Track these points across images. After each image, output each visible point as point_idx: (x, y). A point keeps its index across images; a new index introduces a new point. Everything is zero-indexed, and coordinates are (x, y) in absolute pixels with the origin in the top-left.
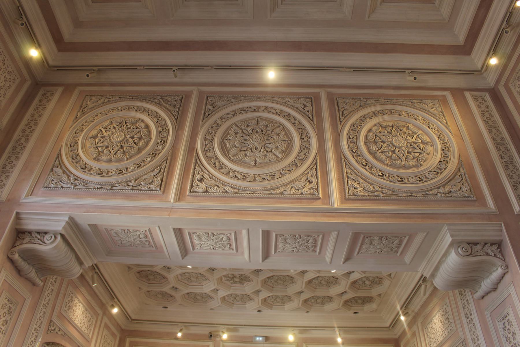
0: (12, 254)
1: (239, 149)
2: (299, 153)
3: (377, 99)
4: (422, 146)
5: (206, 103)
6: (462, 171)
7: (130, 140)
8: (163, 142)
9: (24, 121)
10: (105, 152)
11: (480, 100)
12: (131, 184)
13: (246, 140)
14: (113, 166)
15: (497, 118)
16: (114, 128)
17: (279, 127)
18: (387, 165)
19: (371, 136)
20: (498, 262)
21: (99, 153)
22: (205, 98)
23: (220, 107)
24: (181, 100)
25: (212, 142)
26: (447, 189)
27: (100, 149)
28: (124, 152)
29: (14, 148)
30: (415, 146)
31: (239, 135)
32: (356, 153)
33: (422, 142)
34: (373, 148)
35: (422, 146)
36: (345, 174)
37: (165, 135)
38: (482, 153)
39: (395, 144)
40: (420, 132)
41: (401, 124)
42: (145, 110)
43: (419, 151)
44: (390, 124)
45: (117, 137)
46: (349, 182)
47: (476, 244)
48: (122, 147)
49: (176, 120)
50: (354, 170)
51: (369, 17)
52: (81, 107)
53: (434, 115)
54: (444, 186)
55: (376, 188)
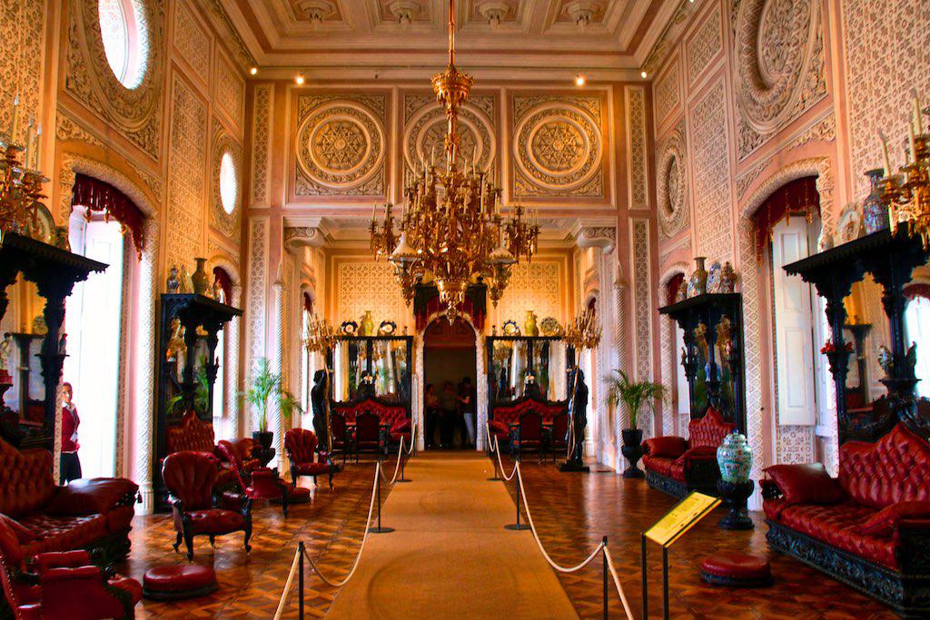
5: (406, 106)
6: (600, 173)
9: (254, 128)
11: (635, 96)
12: (361, 189)
14: (343, 173)
15: (643, 118)
16: (335, 134)
18: (546, 167)
19: (538, 140)
20: (611, 240)
21: (330, 161)
26: (585, 189)
27: (329, 156)
29: (257, 157)
33: (577, 145)
34: (538, 151)
35: (575, 148)
38: (620, 152)
40: (577, 134)
42: (355, 113)
45: (340, 145)
47: (599, 228)
48: (346, 155)
50: (521, 173)
53: (591, 115)
55: (536, 189)
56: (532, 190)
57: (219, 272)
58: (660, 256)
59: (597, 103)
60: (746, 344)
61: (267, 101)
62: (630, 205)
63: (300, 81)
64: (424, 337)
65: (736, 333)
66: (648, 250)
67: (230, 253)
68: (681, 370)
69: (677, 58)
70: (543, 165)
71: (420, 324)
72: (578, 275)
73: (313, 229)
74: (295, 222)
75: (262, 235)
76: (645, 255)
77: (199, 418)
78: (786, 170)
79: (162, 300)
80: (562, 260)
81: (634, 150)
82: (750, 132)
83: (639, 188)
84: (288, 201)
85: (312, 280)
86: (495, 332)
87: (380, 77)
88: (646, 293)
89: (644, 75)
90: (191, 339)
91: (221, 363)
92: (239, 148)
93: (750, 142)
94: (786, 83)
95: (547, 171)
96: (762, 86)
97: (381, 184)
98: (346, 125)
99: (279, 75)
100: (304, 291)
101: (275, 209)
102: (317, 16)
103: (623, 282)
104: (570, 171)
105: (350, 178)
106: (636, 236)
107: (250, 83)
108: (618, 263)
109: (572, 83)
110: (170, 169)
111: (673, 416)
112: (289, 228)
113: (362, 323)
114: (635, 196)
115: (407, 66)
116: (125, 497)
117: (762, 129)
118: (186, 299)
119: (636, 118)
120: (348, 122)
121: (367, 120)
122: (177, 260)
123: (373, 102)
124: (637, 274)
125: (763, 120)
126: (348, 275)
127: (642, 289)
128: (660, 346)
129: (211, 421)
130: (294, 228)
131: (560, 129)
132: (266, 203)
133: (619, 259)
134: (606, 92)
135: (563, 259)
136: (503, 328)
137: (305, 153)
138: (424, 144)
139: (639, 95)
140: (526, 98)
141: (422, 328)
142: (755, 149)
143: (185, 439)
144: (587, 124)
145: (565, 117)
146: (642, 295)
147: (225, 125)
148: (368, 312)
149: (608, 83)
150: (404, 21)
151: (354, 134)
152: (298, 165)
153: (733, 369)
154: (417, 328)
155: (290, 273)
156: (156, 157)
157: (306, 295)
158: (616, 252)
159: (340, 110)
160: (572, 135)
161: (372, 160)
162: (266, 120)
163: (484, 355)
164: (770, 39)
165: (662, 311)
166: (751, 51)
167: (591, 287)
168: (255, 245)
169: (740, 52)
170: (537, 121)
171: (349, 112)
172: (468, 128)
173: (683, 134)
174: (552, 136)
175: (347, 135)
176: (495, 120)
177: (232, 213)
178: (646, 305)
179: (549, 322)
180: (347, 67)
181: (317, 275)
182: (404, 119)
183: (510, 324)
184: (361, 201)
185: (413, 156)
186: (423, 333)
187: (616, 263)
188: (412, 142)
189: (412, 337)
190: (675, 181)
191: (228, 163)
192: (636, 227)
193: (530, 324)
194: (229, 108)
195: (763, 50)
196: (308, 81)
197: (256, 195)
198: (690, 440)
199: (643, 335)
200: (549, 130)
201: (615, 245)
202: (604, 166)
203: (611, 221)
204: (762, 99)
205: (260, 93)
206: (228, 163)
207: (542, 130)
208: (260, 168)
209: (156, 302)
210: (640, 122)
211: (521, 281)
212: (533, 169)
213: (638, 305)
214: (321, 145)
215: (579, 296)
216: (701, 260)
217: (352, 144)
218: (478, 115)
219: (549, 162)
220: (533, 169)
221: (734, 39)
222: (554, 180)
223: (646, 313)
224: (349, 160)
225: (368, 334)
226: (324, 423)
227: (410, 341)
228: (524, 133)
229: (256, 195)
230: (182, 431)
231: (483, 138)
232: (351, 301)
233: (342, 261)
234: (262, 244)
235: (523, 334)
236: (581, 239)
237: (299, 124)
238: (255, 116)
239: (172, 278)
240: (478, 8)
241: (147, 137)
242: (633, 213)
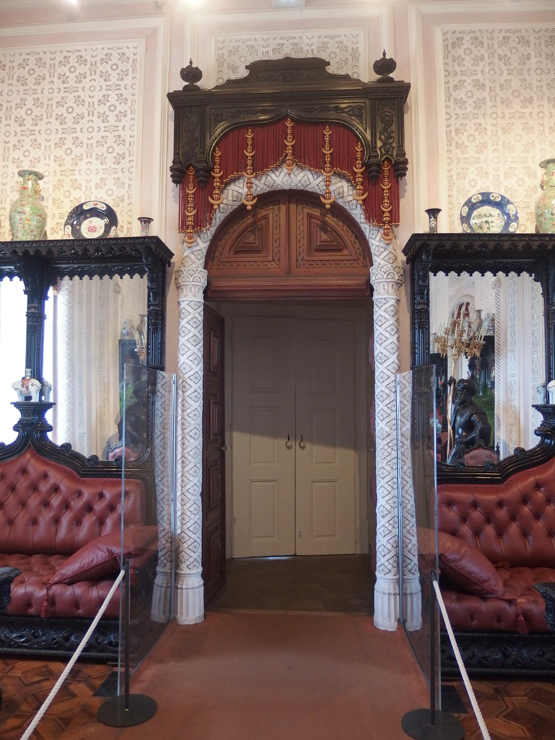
71: (191, 213)
163: (397, 312)
186: (202, 244)
211: (515, 84)
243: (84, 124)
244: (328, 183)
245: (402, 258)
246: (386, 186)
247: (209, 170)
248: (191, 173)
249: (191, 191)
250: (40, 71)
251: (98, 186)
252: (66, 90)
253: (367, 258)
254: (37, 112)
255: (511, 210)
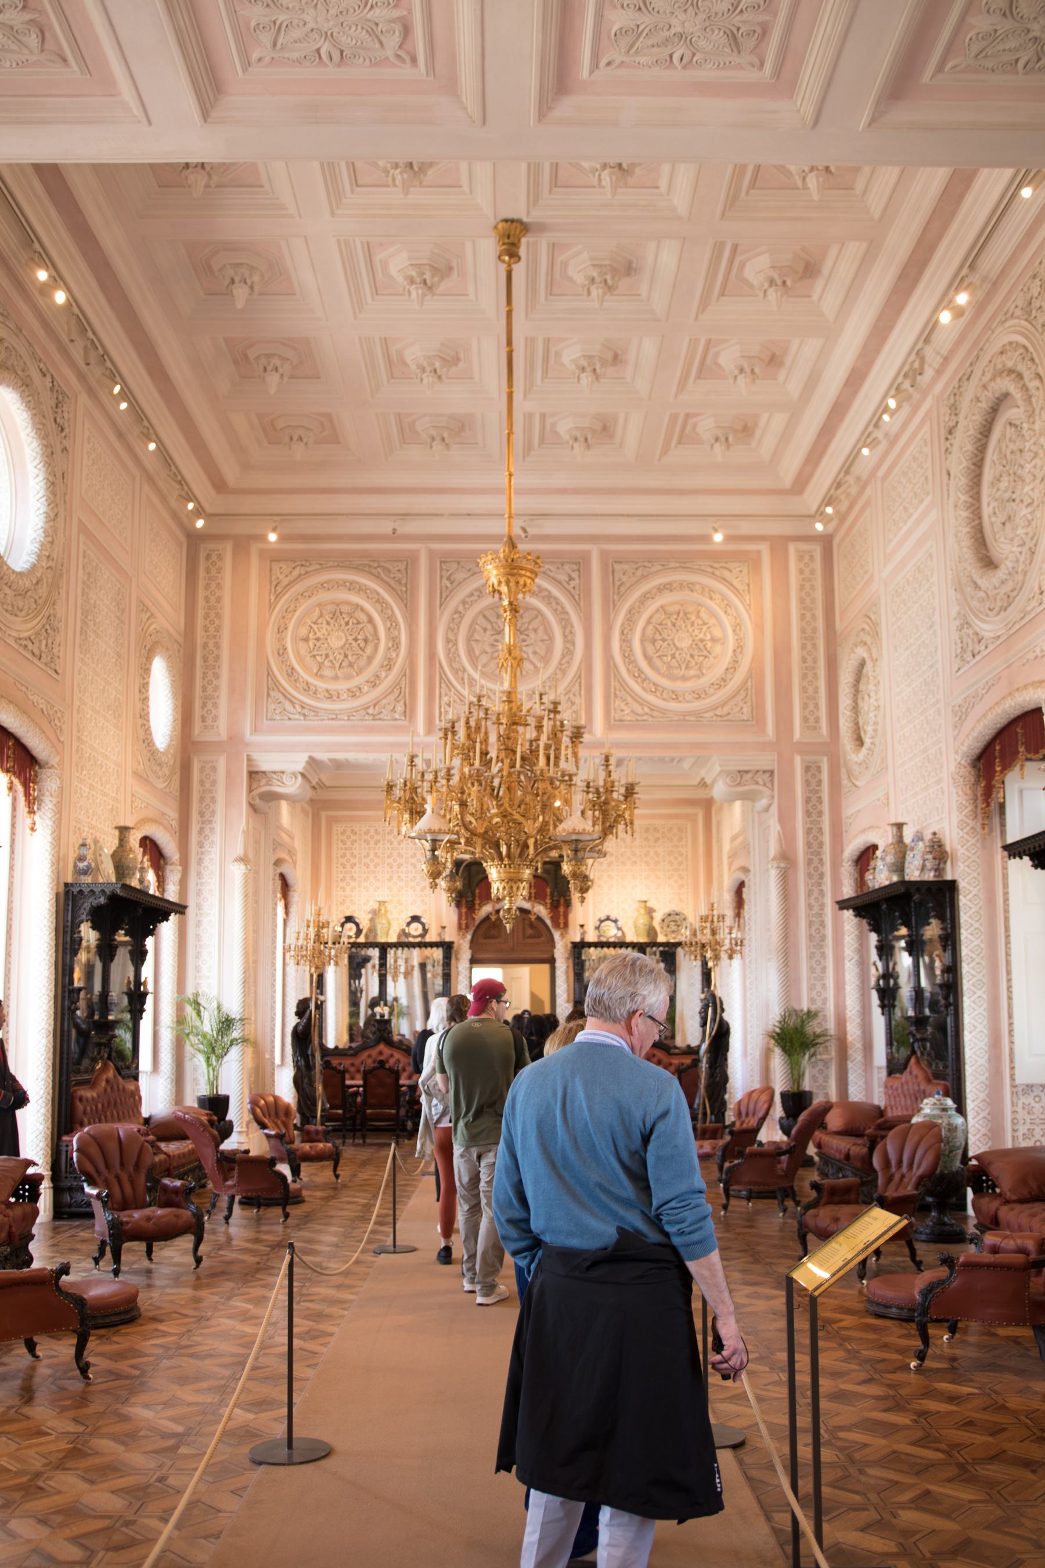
0: (253, 799)
1: (489, 655)
2: (562, 659)
3: (664, 561)
4: (709, 645)
5: (441, 577)
6: (749, 683)
7: (354, 644)
8: (397, 646)
9: (200, 613)
10: (327, 663)
11: (806, 558)
12: (371, 711)
13: (497, 641)
14: (342, 686)
15: (819, 594)
16: (328, 623)
17: (537, 617)
18: (663, 675)
20: (767, 791)
21: (321, 666)
22: (438, 564)
23: (460, 583)
24: (406, 569)
25: (456, 644)
26: (726, 710)
27: (319, 658)
28: (351, 665)
29: (205, 659)
30: (701, 645)
31: (488, 633)
32: (628, 657)
33: (714, 640)
36: (613, 690)
37: (396, 633)
39: (677, 644)
40: (713, 621)
41: (690, 609)
42: (361, 589)
43: (705, 653)
44: (676, 608)
45: (337, 640)
46: (617, 703)
47: (747, 772)
48: (346, 656)
49: (406, 605)
51: (660, 460)
52: (271, 583)
54: (722, 706)
55: (647, 710)
56: (639, 710)
57: (149, 844)
58: (844, 816)
59: (745, 571)
60: (964, 959)
61: (219, 570)
62: (797, 735)
63: (273, 537)
64: (472, 941)
65: (950, 940)
66: (826, 807)
67: (163, 814)
68: (874, 996)
69: (867, 503)
70: (659, 673)
71: (464, 922)
72: (719, 841)
73: (294, 774)
74: (266, 762)
75: (214, 783)
76: (820, 814)
77: (120, 1074)
78: (1016, 694)
79: (67, 893)
80: (693, 818)
81: (803, 647)
82: (970, 632)
83: (811, 706)
84: (255, 730)
85: (291, 852)
86: (583, 934)
87: (399, 531)
88: (822, 876)
89: (819, 527)
90: (106, 951)
91: (150, 987)
92: (176, 646)
93: (970, 648)
94: (1017, 561)
95: (663, 682)
96: (988, 563)
97: (402, 703)
98: (345, 608)
99: (241, 528)
100: (279, 871)
101: (235, 740)
102: (300, 439)
103: (786, 859)
104: (703, 680)
105: (353, 694)
106: (807, 783)
107: (194, 540)
108: (778, 828)
109: (707, 539)
110: (76, 688)
111: (865, 1070)
112: (257, 773)
113: (372, 920)
114: (805, 720)
115: (442, 515)
116: (25, 1190)
117: (988, 628)
118: (103, 891)
119: (808, 594)
120: (348, 603)
121: (379, 601)
122: (86, 829)
123: (389, 571)
124: (809, 845)
125: (987, 615)
126: (348, 843)
127: (816, 869)
128: (844, 959)
129: (136, 1078)
130: (264, 773)
131: (685, 614)
132: (222, 730)
133: (781, 820)
134: (759, 552)
135: (696, 815)
136: (597, 928)
137: (282, 652)
138: (469, 639)
139: (812, 558)
140: (629, 565)
141: (467, 927)
142: (978, 658)
143: (100, 1105)
144: (728, 606)
145: (695, 594)
146: (816, 877)
147: (153, 609)
148: (382, 903)
149: (763, 538)
150: (437, 446)
151: (359, 623)
152: (270, 673)
153: (946, 998)
154: (460, 927)
155: (257, 842)
156: (56, 671)
157: (282, 877)
158: (774, 809)
159: (339, 585)
160: (705, 624)
161: (389, 665)
162: (219, 600)
163: (567, 972)
164: (998, 490)
165: (843, 905)
166: (972, 505)
167: (739, 862)
168: (202, 799)
169: (956, 506)
170: (649, 602)
171: (351, 586)
172: (539, 612)
173: (875, 625)
174: (674, 625)
175: (347, 624)
176: (581, 598)
177: (169, 746)
178: (822, 893)
179: (674, 919)
180: (347, 515)
181: (298, 845)
182: (440, 596)
183: (608, 923)
184: (370, 730)
185: (452, 657)
186: (469, 937)
187: (774, 827)
188: (451, 637)
189: (452, 943)
190: (866, 697)
191: (159, 668)
192: (807, 769)
193: (643, 921)
194: (160, 577)
195: (989, 505)
196: (282, 538)
197: (204, 719)
198: (886, 1107)
199: (817, 941)
200: (669, 615)
201: (773, 797)
202: (755, 673)
203: (766, 760)
204: (988, 581)
205: (208, 557)
206: (159, 668)
207: (657, 615)
208: (210, 676)
209: (57, 895)
210: (813, 601)
212: (640, 676)
213: (809, 893)
214: (306, 640)
215: (721, 876)
216: (899, 826)
217: (356, 640)
218: (556, 592)
219: (669, 667)
220: (640, 676)
221: (948, 485)
222: (676, 696)
223: (822, 907)
224: (351, 665)
225: (382, 939)
226: (311, 1083)
227: (448, 948)
228: (628, 620)
229: (204, 719)
230: (95, 1095)
231: (564, 628)
232: (353, 884)
233: (337, 820)
234: (213, 798)
235: (630, 938)
236: (719, 790)
237: (272, 606)
238: (201, 593)
239: (81, 859)
240: (553, 425)
241: (44, 642)
242: (802, 748)
243: (403, 868)
244: (533, 907)
245: (570, 945)
246: (562, 909)
247: (473, 901)
248: (464, 901)
249: (464, 910)
250: (377, 837)
251: (412, 904)
252: (393, 849)
253: (553, 946)
254: (377, 860)
255: (619, 924)
